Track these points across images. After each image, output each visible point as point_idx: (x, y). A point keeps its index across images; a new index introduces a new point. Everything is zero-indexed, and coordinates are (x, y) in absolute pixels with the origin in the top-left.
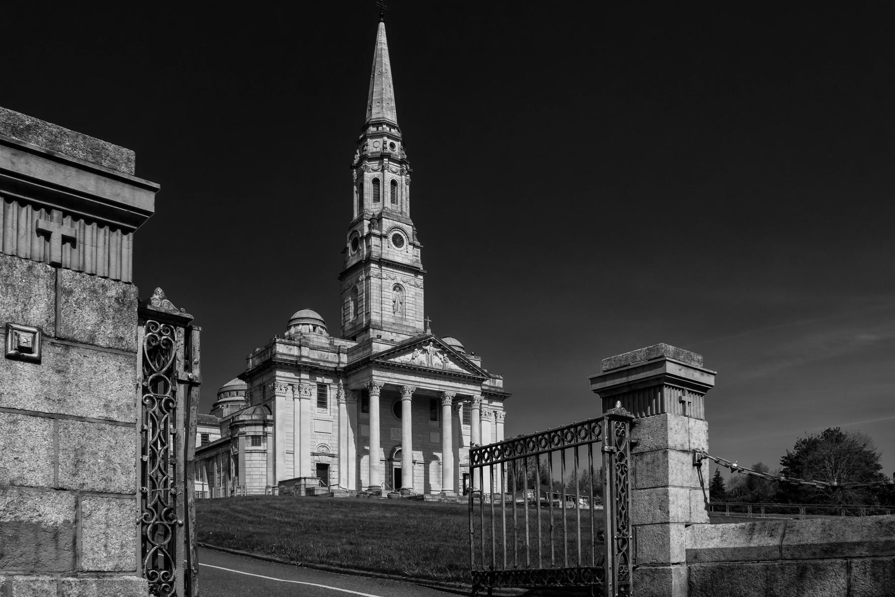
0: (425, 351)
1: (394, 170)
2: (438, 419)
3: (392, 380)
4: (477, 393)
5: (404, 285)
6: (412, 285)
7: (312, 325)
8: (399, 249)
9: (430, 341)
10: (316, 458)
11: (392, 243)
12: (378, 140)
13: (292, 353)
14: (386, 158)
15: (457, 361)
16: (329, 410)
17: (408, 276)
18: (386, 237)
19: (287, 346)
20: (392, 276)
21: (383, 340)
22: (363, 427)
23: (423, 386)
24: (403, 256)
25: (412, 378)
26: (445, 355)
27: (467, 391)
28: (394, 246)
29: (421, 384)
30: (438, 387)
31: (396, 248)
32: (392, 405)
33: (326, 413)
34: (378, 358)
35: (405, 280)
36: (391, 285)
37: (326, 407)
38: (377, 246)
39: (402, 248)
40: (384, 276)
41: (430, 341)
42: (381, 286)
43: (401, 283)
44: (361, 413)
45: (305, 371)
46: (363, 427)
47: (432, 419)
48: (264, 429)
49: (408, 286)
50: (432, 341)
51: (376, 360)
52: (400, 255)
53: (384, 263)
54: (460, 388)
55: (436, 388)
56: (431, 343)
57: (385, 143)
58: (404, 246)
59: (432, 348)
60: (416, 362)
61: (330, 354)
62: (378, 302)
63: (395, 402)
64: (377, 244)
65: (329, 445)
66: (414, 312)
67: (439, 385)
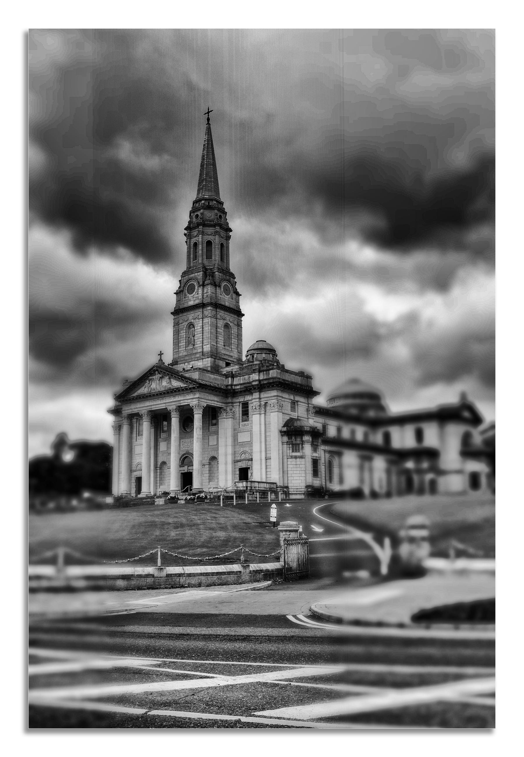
1: (196, 234)
4: (194, 400)
27: (186, 401)
30: (164, 405)
36: (185, 326)
41: (155, 371)
50: (156, 371)
54: (180, 400)
55: (163, 406)
58: (195, 291)
67: (165, 403)
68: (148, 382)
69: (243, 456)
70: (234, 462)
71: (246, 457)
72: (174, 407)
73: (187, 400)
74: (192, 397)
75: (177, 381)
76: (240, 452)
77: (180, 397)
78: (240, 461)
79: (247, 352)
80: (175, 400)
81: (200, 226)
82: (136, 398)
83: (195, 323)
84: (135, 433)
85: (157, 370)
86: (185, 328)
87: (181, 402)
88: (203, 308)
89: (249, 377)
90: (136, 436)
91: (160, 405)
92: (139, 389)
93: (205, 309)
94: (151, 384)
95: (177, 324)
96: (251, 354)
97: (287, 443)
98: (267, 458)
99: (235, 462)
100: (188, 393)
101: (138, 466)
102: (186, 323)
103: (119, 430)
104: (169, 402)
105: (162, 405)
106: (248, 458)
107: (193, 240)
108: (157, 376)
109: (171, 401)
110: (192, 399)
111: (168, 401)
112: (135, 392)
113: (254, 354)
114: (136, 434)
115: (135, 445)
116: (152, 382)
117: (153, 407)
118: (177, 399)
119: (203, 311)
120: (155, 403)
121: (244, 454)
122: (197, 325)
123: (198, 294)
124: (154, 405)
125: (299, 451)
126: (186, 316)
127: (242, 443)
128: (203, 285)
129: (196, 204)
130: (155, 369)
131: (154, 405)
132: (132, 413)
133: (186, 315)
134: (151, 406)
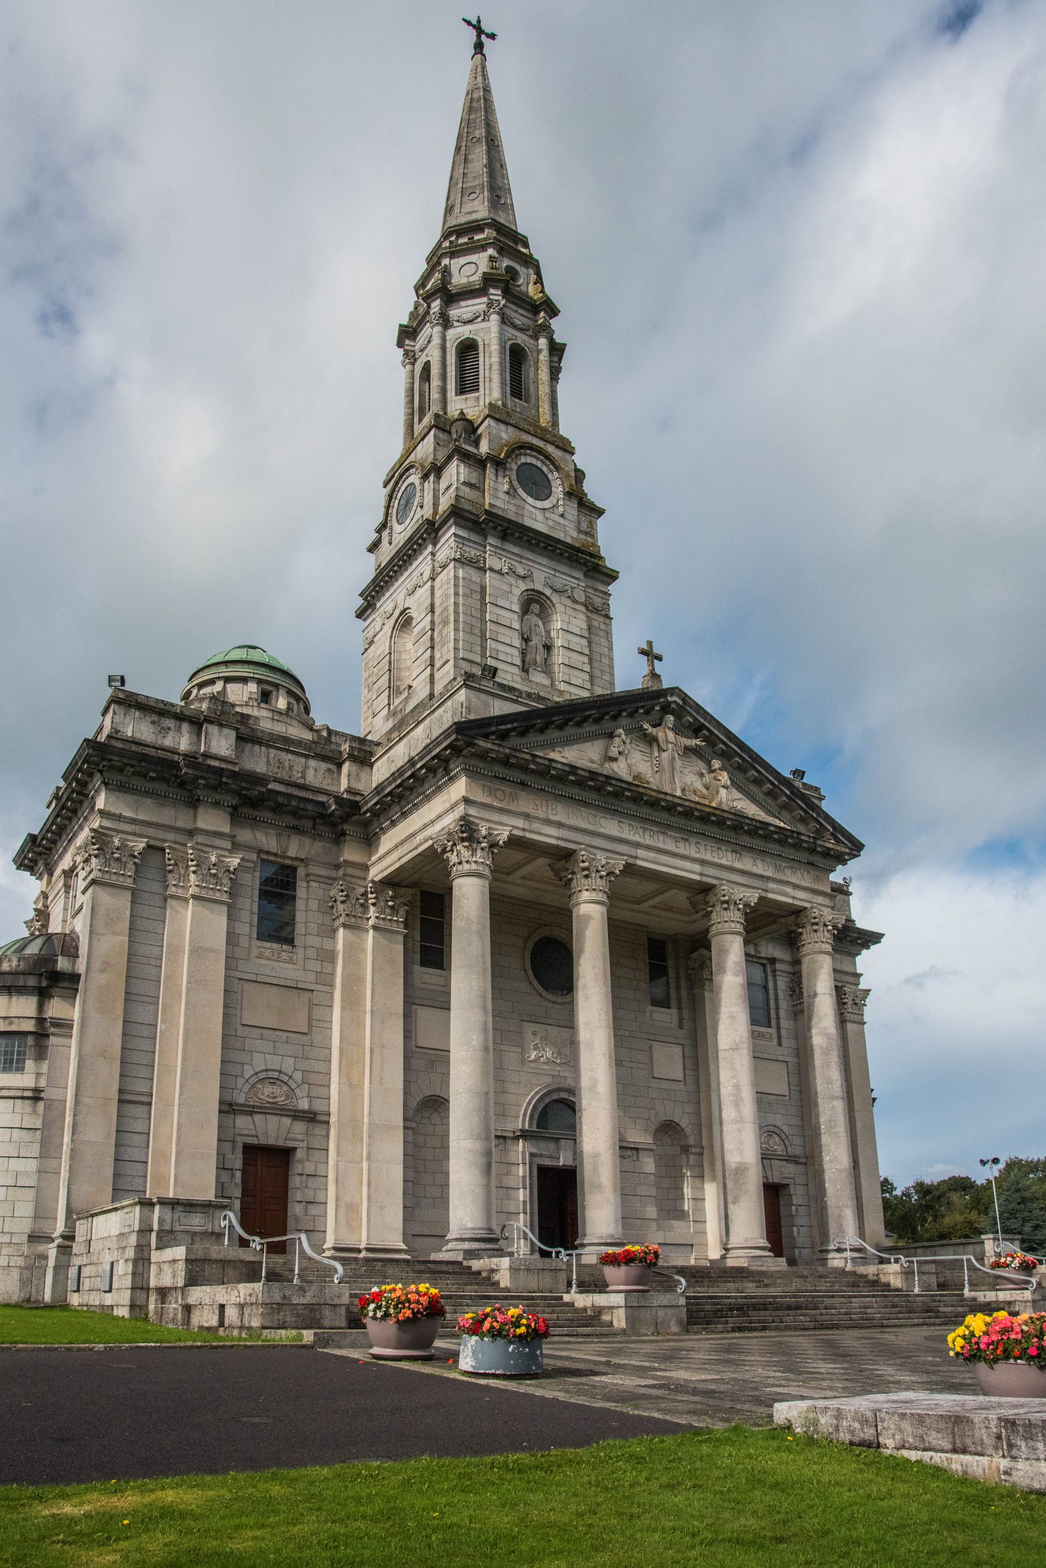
0: (651, 741)
2: (673, 1002)
3: (536, 826)
4: (820, 900)
5: (555, 598)
6: (575, 602)
7: (259, 682)
8: (539, 504)
10: (242, 1122)
11: (515, 483)
12: (473, 258)
13: (168, 742)
15: (754, 789)
16: (300, 951)
17: (573, 580)
18: (499, 464)
19: (155, 718)
20: (521, 571)
21: (502, 687)
22: (424, 1015)
24: (550, 523)
25: (611, 826)
26: (716, 764)
27: (789, 890)
28: (520, 491)
30: (697, 867)
31: (530, 500)
32: (523, 957)
33: (291, 961)
35: (559, 586)
36: (517, 592)
37: (290, 941)
39: (547, 504)
40: (492, 562)
42: (483, 589)
43: (548, 592)
44: (418, 969)
45: (217, 804)
46: (424, 1015)
47: (655, 1003)
48: (41, 1007)
49: (568, 602)
50: (673, 712)
54: (768, 879)
55: (691, 871)
56: (670, 719)
59: (671, 735)
60: (621, 769)
61: (313, 763)
62: (477, 631)
63: (536, 937)
64: (473, 481)
65: (298, 1076)
66: (586, 677)
67: (703, 862)
72: (753, 897)
73: (796, 886)
74: (810, 885)
75: (741, 796)
77: (759, 863)
80: (738, 865)
82: (580, 784)
85: (679, 713)
86: (515, 599)
87: (771, 885)
91: (679, 863)
92: (568, 742)
93: (590, 583)
100: (793, 864)
101: (259, 1086)
102: (523, 586)
104: (721, 867)
105: (688, 865)
109: (724, 862)
110: (814, 891)
111: (708, 857)
112: (552, 745)
115: (238, 975)
117: (641, 853)
118: (746, 863)
120: (648, 841)
123: (562, 516)
124: (649, 848)
131: (649, 848)
132: (528, 835)
133: (521, 557)
134: (637, 845)
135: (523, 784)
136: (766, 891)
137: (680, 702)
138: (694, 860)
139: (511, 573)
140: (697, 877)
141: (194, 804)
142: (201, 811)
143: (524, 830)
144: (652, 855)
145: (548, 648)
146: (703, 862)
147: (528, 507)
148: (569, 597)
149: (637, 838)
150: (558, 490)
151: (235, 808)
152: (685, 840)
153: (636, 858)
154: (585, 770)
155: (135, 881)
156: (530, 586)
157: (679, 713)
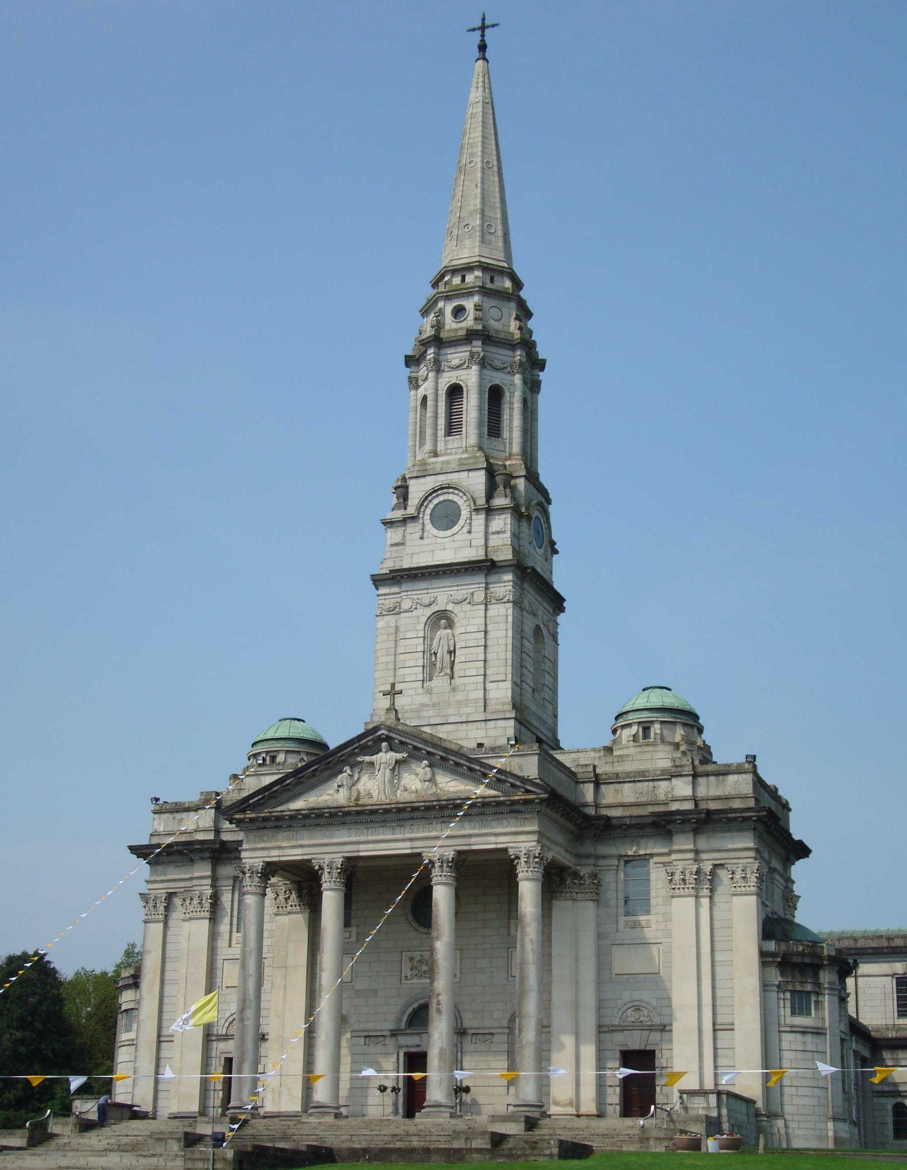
1: (455, 362)
5: (456, 609)
8: (449, 533)
9: (380, 739)
11: (429, 526)
14: (430, 347)
18: (414, 518)
23: (366, 851)
24: (457, 545)
28: (434, 531)
29: (362, 847)
31: (442, 534)
34: (243, 811)
36: (424, 619)
38: (397, 544)
40: (406, 604)
43: (450, 607)
45: (202, 859)
49: (469, 607)
51: (237, 816)
52: (448, 545)
53: (402, 577)
54: (470, 836)
55: (403, 848)
56: (384, 744)
57: (441, 312)
58: (461, 522)
62: (391, 666)
67: (411, 840)
68: (349, 772)
69: (631, 1016)
70: (600, 1032)
71: (641, 1019)
72: (450, 854)
76: (620, 1003)
78: (622, 1029)
79: (617, 718)
81: (476, 339)
83: (461, 615)
84: (227, 920)
85: (388, 739)
86: (421, 626)
88: (486, 575)
89: (654, 787)
90: (231, 932)
91: (392, 845)
93: (493, 578)
94: (359, 779)
95: (390, 611)
96: (639, 723)
97: (778, 986)
98: (717, 1027)
99: (602, 1029)
102: (428, 612)
103: (165, 907)
106: (649, 1023)
107: (448, 378)
108: (385, 757)
113: (652, 722)
114: (231, 924)
116: (360, 772)
119: (487, 584)
120: (370, 838)
121: (633, 1009)
122: (465, 622)
123: (469, 532)
125: (808, 1013)
126: (426, 591)
127: (627, 976)
128: (489, 511)
129: (452, 277)
130: (383, 734)
132: (282, 859)
135: (277, 827)
136: (470, 845)
137: (385, 732)
138: (404, 840)
139: (419, 606)
140: (409, 851)
141: (192, 861)
142: (195, 865)
143: (279, 856)
144: (371, 846)
145: (452, 652)
146: (411, 840)
147: (439, 540)
148: (469, 603)
149: (362, 838)
150: (465, 513)
151: (212, 858)
152: (401, 826)
153: (358, 851)
154: (306, 810)
155: (166, 916)
156: (435, 608)
157: (388, 739)
